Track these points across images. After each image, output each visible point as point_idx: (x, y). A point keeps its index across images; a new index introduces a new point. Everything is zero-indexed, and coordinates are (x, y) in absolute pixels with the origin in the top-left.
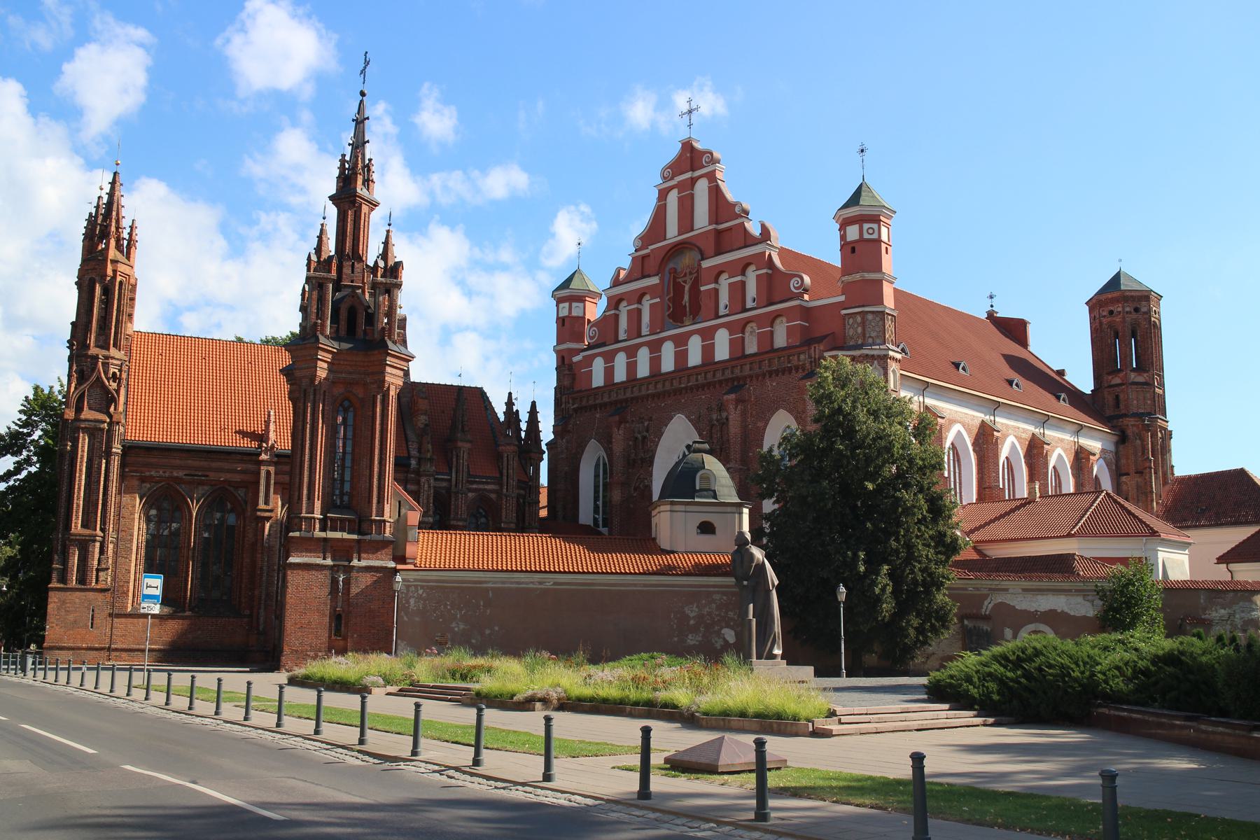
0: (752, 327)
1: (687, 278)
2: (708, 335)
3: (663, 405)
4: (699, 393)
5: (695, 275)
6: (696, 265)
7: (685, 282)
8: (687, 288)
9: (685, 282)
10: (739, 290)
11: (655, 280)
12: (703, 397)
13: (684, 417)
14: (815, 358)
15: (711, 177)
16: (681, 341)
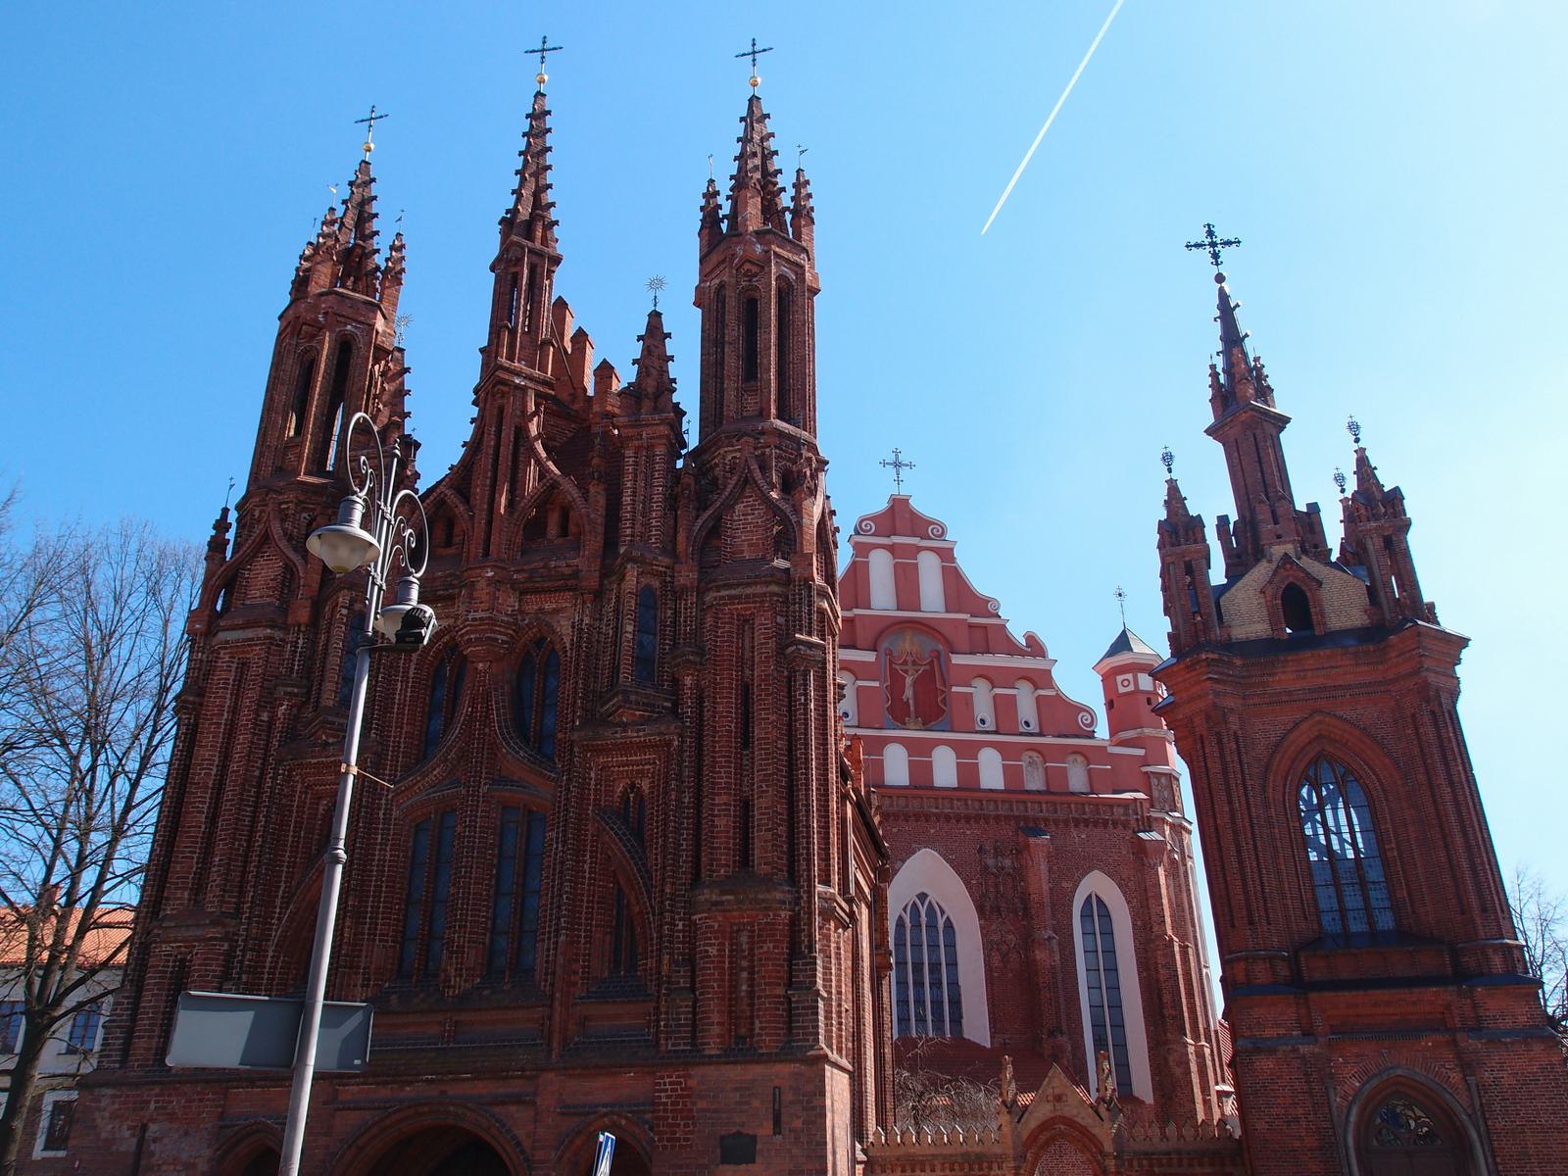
0: (1030, 757)
1: (909, 667)
2: (966, 752)
3: (895, 830)
4: (960, 826)
5: (928, 667)
6: (927, 656)
7: (906, 672)
8: (909, 680)
9: (906, 672)
10: (1005, 708)
11: (869, 657)
12: (968, 832)
13: (936, 853)
14: (1143, 817)
15: (946, 555)
16: (919, 751)
